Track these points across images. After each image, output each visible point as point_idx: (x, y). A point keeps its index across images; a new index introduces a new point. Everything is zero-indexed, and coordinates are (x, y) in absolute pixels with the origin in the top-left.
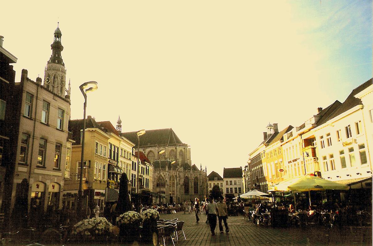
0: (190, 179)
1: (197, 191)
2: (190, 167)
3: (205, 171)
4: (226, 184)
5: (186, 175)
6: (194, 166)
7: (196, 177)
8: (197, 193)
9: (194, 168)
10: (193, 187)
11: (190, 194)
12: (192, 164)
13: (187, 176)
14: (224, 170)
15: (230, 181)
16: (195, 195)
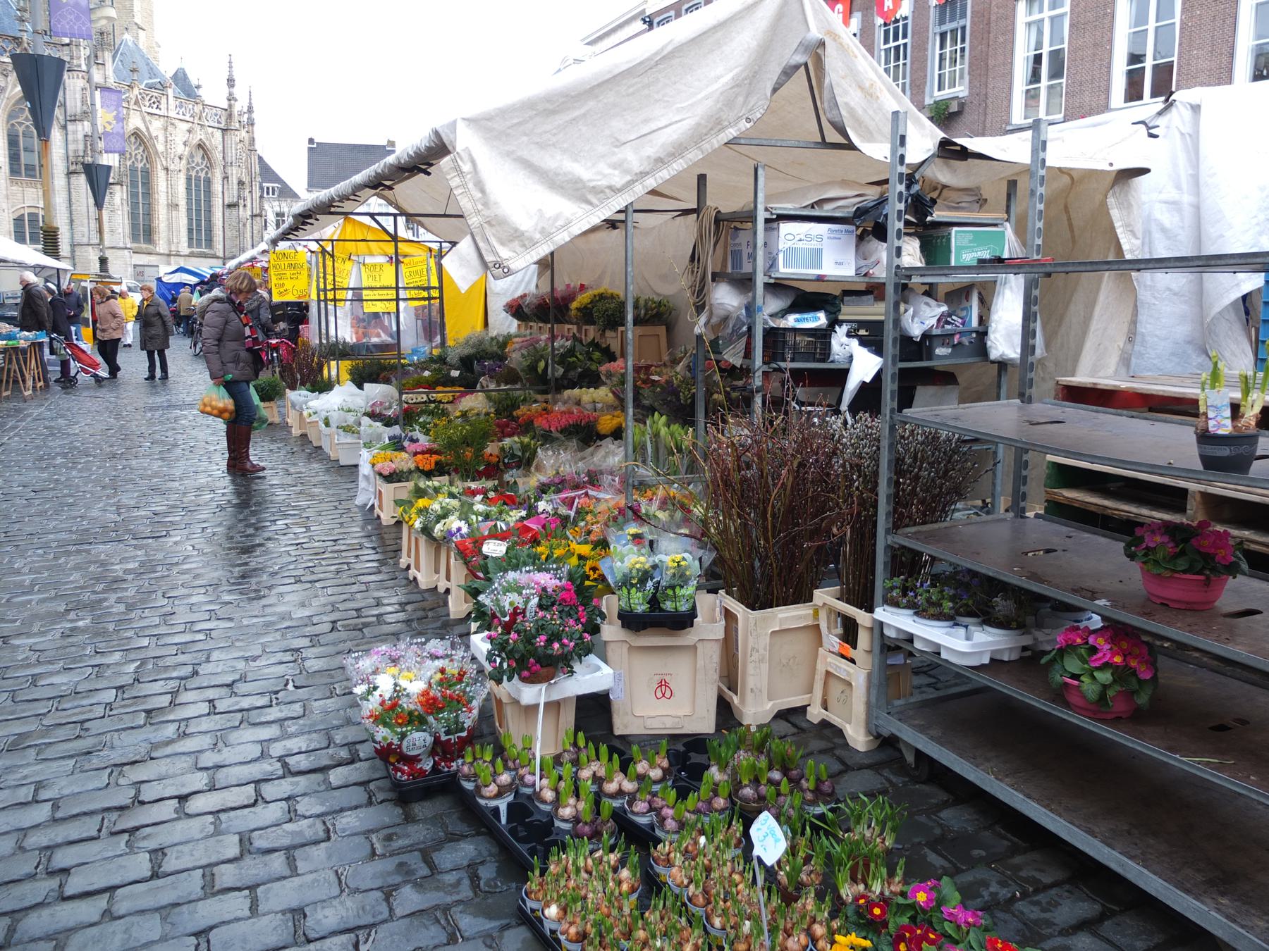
0: (160, 148)
1: (209, 230)
2: (153, 72)
3: (246, 116)
5: (135, 122)
6: (180, 78)
7: (201, 146)
8: (210, 242)
9: (186, 88)
10: (182, 203)
11: (162, 247)
12: (167, 69)
13: (136, 134)
14: (310, 149)
16: (192, 255)
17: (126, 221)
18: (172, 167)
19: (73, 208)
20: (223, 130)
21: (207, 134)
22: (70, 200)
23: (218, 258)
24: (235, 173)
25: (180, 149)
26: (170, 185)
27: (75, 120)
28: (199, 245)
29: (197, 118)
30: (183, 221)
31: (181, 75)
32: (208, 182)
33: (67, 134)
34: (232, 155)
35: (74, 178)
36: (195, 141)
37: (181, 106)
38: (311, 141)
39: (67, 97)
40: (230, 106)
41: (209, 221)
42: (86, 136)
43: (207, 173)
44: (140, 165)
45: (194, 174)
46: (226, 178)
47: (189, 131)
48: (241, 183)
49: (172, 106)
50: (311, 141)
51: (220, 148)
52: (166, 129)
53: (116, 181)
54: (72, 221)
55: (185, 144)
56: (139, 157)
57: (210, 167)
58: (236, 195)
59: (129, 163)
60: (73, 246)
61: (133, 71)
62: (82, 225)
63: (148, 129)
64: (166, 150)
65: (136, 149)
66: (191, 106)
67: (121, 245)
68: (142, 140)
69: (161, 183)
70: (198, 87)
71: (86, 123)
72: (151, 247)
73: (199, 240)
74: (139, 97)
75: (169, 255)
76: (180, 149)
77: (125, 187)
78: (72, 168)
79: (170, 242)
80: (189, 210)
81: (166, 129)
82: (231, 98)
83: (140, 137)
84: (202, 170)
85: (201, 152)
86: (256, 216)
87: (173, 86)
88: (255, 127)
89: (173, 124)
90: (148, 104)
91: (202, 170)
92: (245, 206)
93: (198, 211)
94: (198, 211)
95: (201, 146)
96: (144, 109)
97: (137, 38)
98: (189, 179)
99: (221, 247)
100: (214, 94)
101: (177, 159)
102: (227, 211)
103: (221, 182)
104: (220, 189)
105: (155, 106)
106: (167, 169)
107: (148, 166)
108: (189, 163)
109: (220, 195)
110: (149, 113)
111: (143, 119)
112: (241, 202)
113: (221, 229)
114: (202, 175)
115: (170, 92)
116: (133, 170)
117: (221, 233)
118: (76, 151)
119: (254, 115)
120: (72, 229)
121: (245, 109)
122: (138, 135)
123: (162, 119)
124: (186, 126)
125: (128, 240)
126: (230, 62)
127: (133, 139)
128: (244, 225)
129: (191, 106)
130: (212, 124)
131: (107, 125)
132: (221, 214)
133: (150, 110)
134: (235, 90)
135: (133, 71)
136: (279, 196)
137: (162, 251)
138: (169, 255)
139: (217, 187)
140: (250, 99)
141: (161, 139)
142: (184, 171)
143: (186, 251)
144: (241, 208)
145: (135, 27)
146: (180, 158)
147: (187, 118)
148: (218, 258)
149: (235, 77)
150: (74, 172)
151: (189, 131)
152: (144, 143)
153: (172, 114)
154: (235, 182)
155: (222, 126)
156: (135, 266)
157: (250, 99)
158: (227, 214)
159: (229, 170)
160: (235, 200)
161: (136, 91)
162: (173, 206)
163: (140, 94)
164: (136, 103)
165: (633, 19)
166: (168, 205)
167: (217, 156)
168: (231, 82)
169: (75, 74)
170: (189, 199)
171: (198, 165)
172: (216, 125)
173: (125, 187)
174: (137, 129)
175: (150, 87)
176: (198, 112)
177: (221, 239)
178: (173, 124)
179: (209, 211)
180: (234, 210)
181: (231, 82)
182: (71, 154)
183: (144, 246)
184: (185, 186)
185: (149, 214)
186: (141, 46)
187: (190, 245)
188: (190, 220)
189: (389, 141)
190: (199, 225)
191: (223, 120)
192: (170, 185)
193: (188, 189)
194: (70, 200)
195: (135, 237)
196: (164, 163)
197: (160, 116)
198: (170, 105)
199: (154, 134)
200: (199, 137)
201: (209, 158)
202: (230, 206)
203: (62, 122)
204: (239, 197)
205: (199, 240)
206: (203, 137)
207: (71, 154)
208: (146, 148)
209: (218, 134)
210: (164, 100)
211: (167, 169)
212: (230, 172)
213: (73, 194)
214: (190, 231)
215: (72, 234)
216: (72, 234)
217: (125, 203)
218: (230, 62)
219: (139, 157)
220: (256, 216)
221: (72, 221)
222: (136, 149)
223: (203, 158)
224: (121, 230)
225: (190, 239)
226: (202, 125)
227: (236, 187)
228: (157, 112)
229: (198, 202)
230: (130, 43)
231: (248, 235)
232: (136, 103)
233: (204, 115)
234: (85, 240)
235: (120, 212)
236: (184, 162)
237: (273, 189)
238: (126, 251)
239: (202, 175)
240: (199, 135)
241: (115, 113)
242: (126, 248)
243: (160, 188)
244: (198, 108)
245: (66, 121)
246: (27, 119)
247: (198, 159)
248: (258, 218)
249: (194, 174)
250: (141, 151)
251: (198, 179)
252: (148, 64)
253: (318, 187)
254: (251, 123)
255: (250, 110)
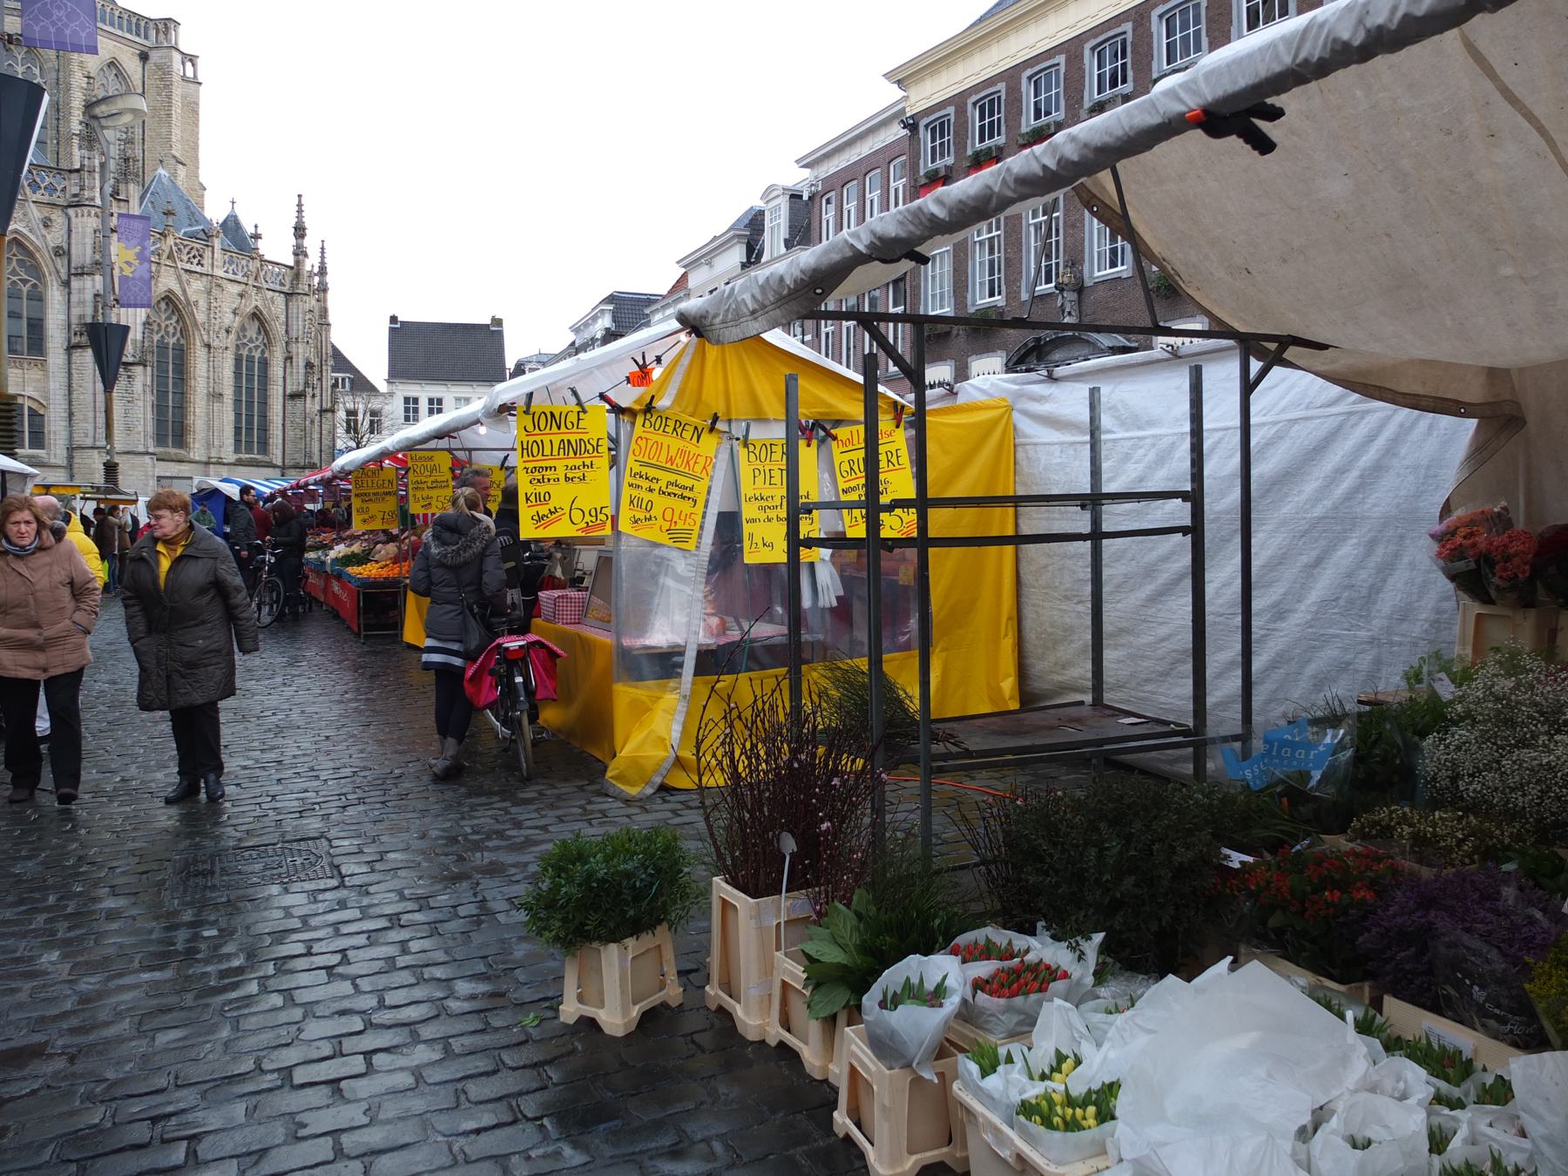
0: (201, 317)
1: (264, 428)
2: (195, 215)
3: (317, 279)
4: (407, 419)
5: (167, 281)
6: (232, 226)
7: (256, 316)
8: (264, 446)
10: (229, 392)
11: (197, 451)
12: (215, 212)
14: (392, 330)
15: (431, 401)
16: (239, 463)
17: (149, 416)
18: (215, 343)
19: (74, 396)
20: (287, 294)
21: (265, 299)
22: (70, 385)
23: (275, 466)
24: (302, 352)
25: (227, 319)
26: (213, 368)
27: (82, 274)
28: (249, 450)
29: (252, 278)
30: (229, 417)
31: (231, 224)
32: (265, 364)
33: (69, 294)
34: (297, 328)
35: (76, 354)
36: (249, 309)
37: (231, 263)
38: (394, 319)
39: (73, 241)
40: (298, 263)
41: (264, 417)
42: (96, 296)
43: (263, 352)
44: (172, 341)
45: (245, 352)
46: (289, 358)
47: (241, 296)
48: (309, 365)
49: (218, 263)
50: (394, 319)
51: (283, 318)
52: (209, 293)
53: (137, 360)
54: (71, 414)
55: (235, 313)
56: (171, 330)
57: (268, 344)
58: (302, 382)
59: (156, 338)
60: (71, 450)
61: (168, 213)
62: (86, 420)
63: (184, 291)
64: (209, 319)
65: (168, 318)
66: (244, 262)
67: (141, 449)
68: (176, 306)
69: (199, 364)
70: (257, 237)
71: (98, 278)
72: (182, 452)
73: (249, 443)
74: (174, 248)
75: (207, 463)
76: (227, 319)
77: (149, 369)
78: (75, 340)
79: (209, 445)
80: (237, 402)
81: (209, 293)
82: (300, 252)
83: (173, 303)
84: (257, 347)
85: (257, 323)
86: (326, 411)
87: (221, 235)
88: (330, 295)
89: (219, 285)
90: (185, 258)
91: (257, 347)
92: (314, 396)
93: (250, 404)
94: (250, 404)
95: (256, 316)
96: (179, 265)
97: (175, 174)
98: (238, 360)
99: (279, 452)
100: (276, 247)
101: (223, 334)
102: (289, 403)
103: (282, 364)
104: (281, 373)
105: (196, 261)
106: (208, 346)
107: (182, 341)
108: (239, 338)
109: (281, 382)
110: (186, 271)
111: (179, 278)
112: (309, 390)
113: (280, 427)
114: (257, 355)
115: (217, 243)
116: (162, 347)
117: (280, 433)
118: (81, 317)
119: (329, 279)
120: (70, 425)
121: (316, 270)
122: (170, 299)
123: (204, 279)
124: (235, 289)
125: (150, 442)
126: (300, 205)
127: (163, 305)
128: (312, 422)
129: (244, 262)
130: (272, 286)
131: (125, 266)
132: (280, 407)
133: (188, 267)
134: (307, 242)
135: (168, 213)
136: (352, 388)
137: (197, 458)
138: (207, 463)
139: (276, 370)
140: (323, 257)
141: (202, 304)
142: (232, 349)
143: (232, 458)
144: (309, 399)
145: (173, 161)
146: (228, 332)
147: (239, 278)
148: (275, 466)
149: (307, 225)
150: (78, 346)
151: (241, 296)
152: (179, 310)
153: (219, 272)
154: (302, 364)
155: (285, 289)
156: (160, 479)
157: (323, 257)
158: (289, 408)
159: (293, 348)
160: (301, 388)
161: (170, 241)
162: (216, 396)
163: (176, 244)
164: (170, 256)
165: (884, 123)
166: (209, 394)
167: (278, 329)
168: (300, 231)
169: (86, 210)
170: (238, 388)
171: (251, 341)
172: (278, 288)
173: (149, 369)
174: (170, 291)
175: (192, 236)
176: (254, 270)
177: (280, 441)
178: (219, 285)
179: (264, 403)
180: (299, 403)
181: (300, 231)
182: (74, 320)
183: (173, 451)
184: (232, 369)
185: (182, 408)
186: (179, 183)
187: (237, 450)
188: (238, 415)
189: (494, 319)
190: (250, 422)
191: (288, 282)
192: (213, 368)
193: (237, 374)
194: (70, 385)
195: (160, 439)
196: (205, 338)
197: (201, 274)
198: (217, 260)
199: (193, 298)
200: (254, 303)
201: (266, 333)
202: (294, 396)
203: (64, 277)
204: (306, 384)
205: (249, 443)
206: (259, 304)
207: (74, 320)
208: (181, 318)
209: (280, 299)
210: (208, 254)
211: (208, 346)
212: (294, 351)
213: (75, 376)
214: (238, 430)
215: (71, 433)
216: (71, 433)
217: (148, 390)
218: (300, 205)
219: (171, 330)
220: (326, 411)
221: (71, 414)
222: (168, 318)
223: (259, 333)
224: (141, 428)
225: (237, 441)
226: (258, 288)
227: (302, 370)
228: (198, 269)
229: (250, 391)
230: (165, 180)
231: (316, 436)
232: (170, 256)
233: (262, 274)
234: (89, 442)
235: (140, 403)
236: (232, 336)
237: (343, 379)
238: (147, 458)
239: (257, 355)
240: (255, 301)
241: (138, 249)
242: (147, 453)
243: (198, 372)
244: (255, 264)
245: (69, 275)
246: (14, 272)
247: (252, 331)
248: (329, 415)
249: (245, 352)
250: (173, 321)
251: (250, 359)
252: (188, 208)
253: (402, 377)
254: (323, 289)
255: (323, 271)
